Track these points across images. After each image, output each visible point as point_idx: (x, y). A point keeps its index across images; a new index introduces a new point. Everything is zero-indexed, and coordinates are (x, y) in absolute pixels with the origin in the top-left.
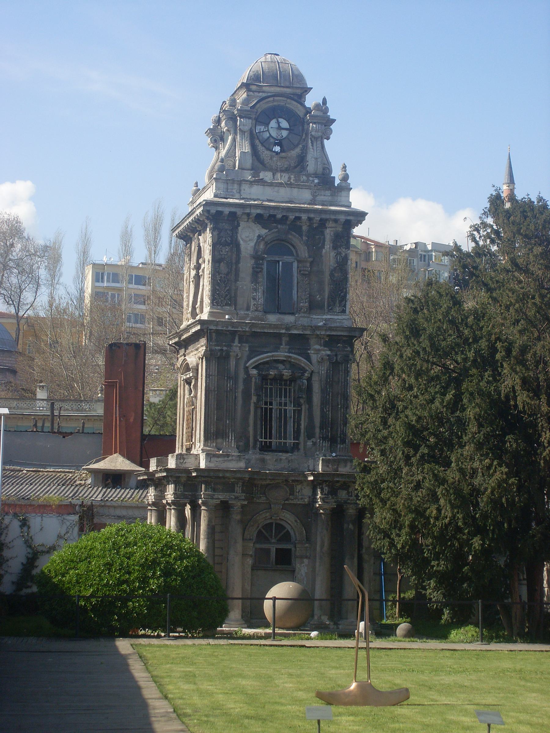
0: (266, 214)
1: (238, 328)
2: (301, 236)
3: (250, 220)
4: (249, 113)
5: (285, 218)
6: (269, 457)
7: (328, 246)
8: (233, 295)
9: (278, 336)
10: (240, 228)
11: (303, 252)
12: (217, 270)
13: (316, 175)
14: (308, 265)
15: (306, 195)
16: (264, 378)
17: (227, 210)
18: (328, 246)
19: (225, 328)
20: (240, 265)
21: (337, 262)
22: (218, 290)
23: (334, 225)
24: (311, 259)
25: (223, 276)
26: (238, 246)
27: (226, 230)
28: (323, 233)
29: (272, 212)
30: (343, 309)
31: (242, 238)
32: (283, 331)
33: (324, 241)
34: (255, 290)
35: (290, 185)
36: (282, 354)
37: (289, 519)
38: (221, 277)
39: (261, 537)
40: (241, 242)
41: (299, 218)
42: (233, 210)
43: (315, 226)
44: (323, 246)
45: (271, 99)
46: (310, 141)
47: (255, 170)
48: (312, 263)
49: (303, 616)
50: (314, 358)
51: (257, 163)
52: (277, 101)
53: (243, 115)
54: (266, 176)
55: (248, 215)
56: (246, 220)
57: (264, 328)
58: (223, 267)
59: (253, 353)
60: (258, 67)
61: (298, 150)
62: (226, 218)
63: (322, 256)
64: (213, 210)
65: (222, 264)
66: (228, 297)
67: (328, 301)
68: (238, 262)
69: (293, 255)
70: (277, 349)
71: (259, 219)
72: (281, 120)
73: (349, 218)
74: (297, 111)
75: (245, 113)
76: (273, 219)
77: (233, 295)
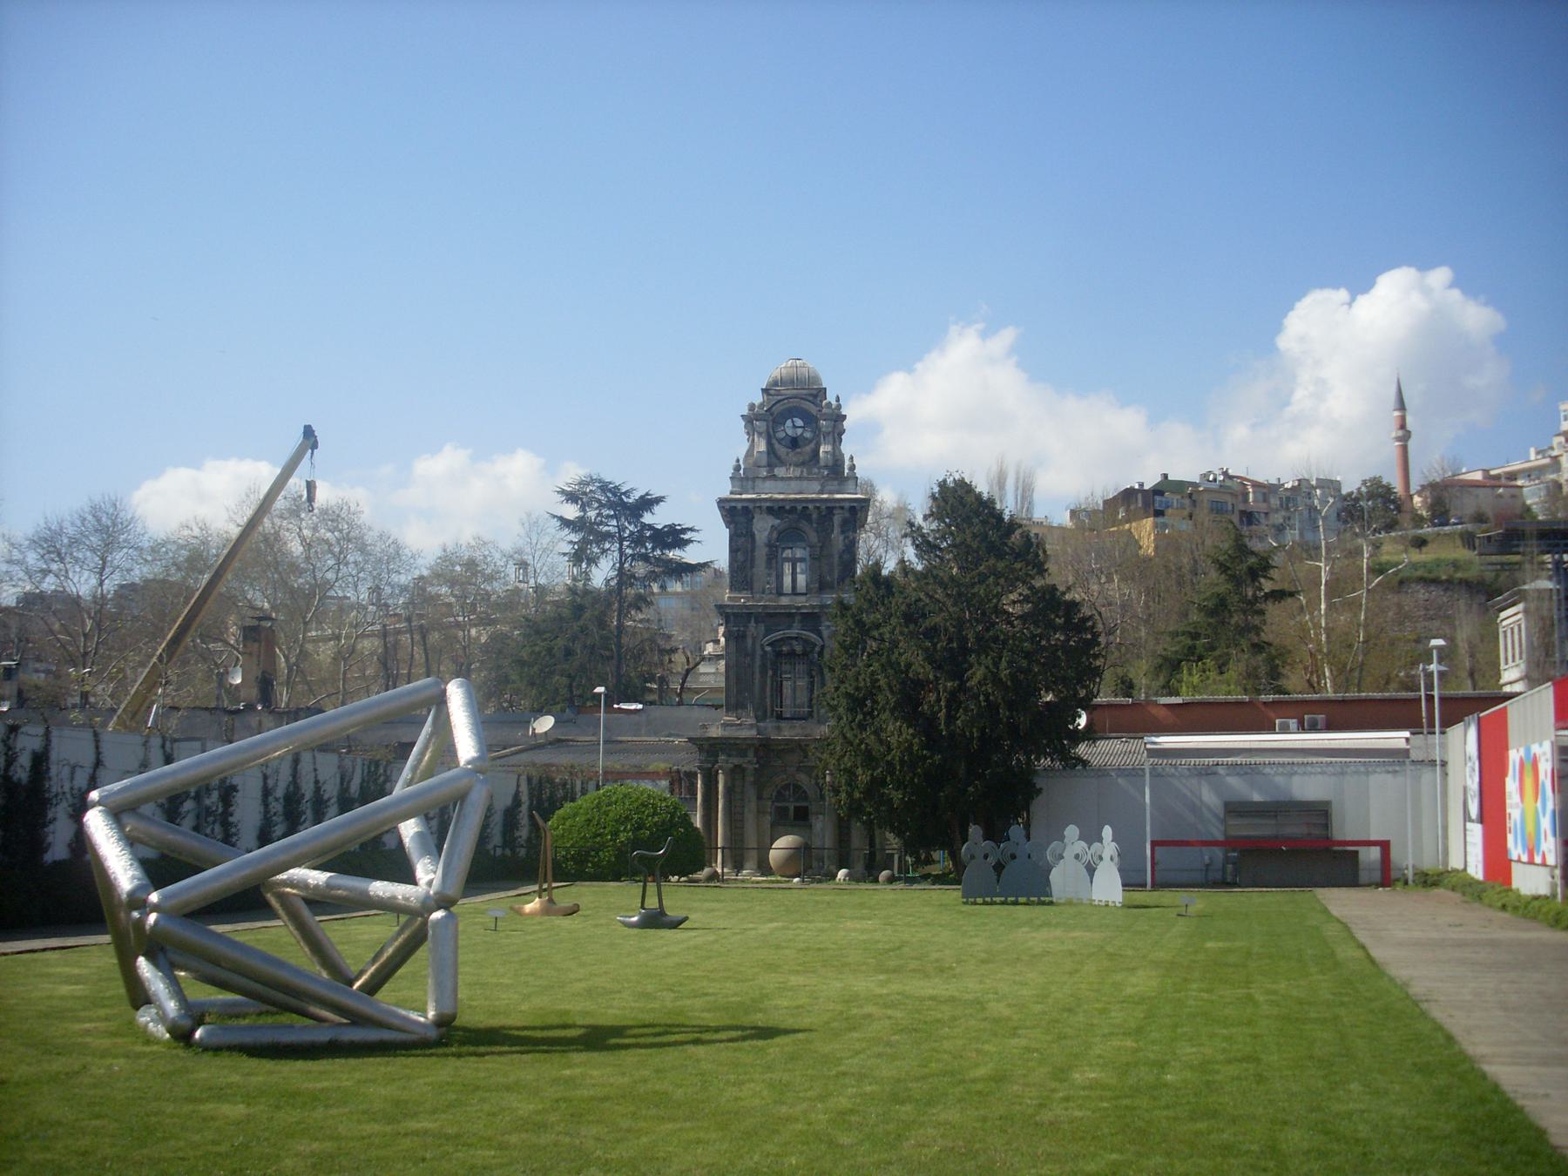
0: (776, 506)
5: (793, 510)
6: (783, 724)
7: (837, 530)
9: (790, 615)
11: (813, 537)
13: (826, 467)
15: (816, 486)
16: (779, 654)
17: (739, 506)
18: (837, 530)
26: (753, 536)
35: (800, 478)
36: (794, 632)
37: (802, 778)
39: (780, 796)
41: (805, 508)
47: (770, 466)
49: (807, 865)
50: (825, 633)
51: (774, 460)
54: (780, 471)
58: (740, 556)
59: (767, 633)
60: (776, 374)
61: (812, 445)
64: (727, 506)
68: (753, 550)
70: (790, 627)
71: (770, 511)
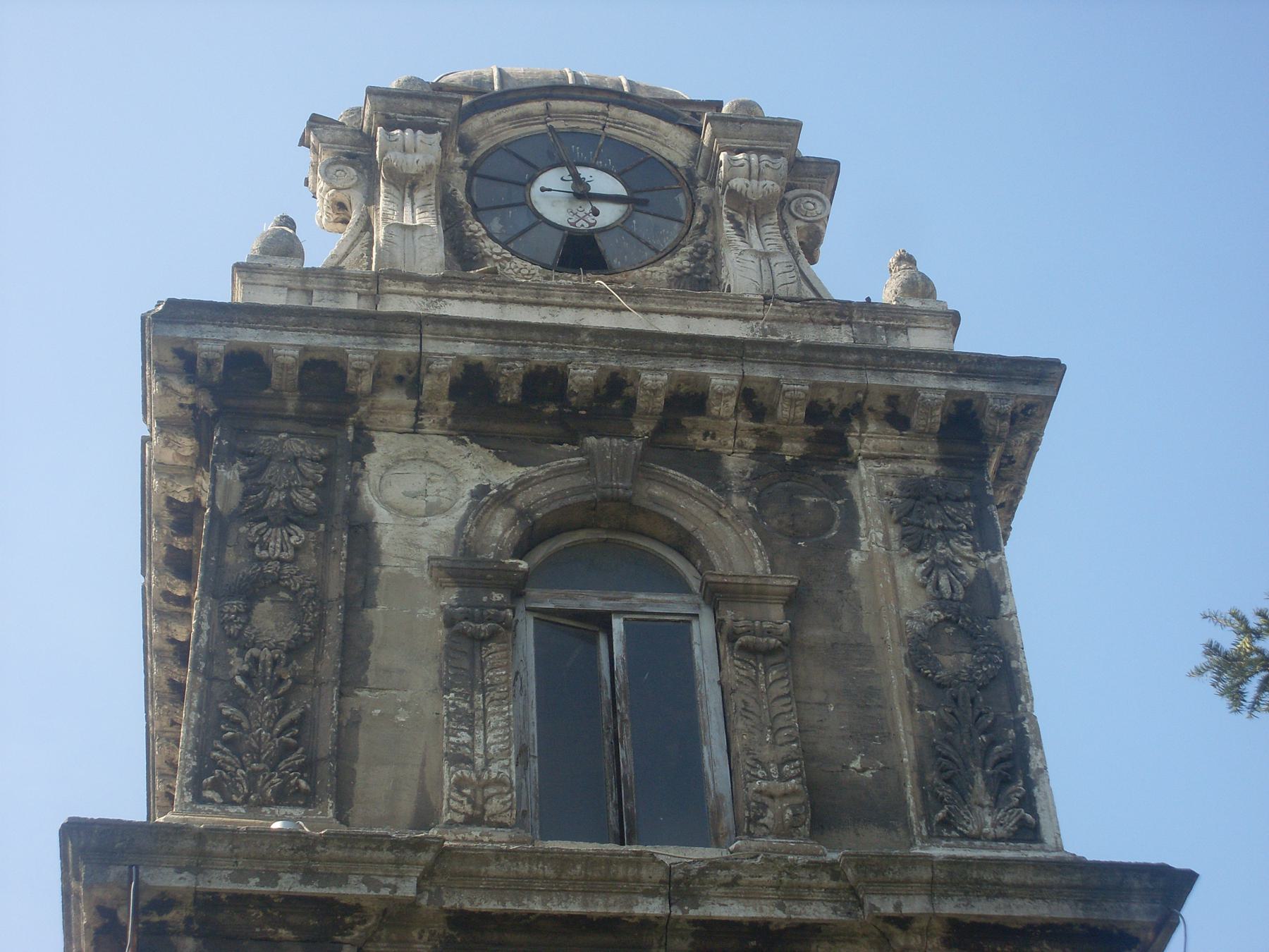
0: (513, 365)
1: (343, 880)
2: (724, 490)
3: (428, 421)
4: (429, 106)
7: (875, 534)
8: (326, 745)
10: (374, 461)
12: (233, 630)
14: (776, 612)
18: (875, 534)
19: (252, 886)
20: (378, 615)
21: (939, 600)
22: (237, 724)
23: (890, 441)
24: (786, 581)
25: (266, 655)
26: (361, 532)
27: (295, 460)
28: (838, 488)
29: (541, 356)
30: (1022, 823)
31: (389, 506)
32: (654, 907)
33: (851, 513)
34: (468, 720)
38: (255, 660)
40: (382, 515)
42: (321, 340)
43: (792, 449)
44: (850, 536)
45: (536, 107)
46: (727, 225)
48: (795, 601)
52: (567, 116)
53: (401, 117)
55: (411, 378)
56: (406, 420)
57: (523, 886)
62: (291, 406)
63: (845, 578)
64: (212, 342)
65: (264, 606)
66: (296, 758)
67: (921, 782)
68: (360, 593)
69: (686, 589)
72: (584, 172)
73: (965, 385)
74: (657, 147)
75: (408, 104)
76: (552, 409)
77: (326, 745)
